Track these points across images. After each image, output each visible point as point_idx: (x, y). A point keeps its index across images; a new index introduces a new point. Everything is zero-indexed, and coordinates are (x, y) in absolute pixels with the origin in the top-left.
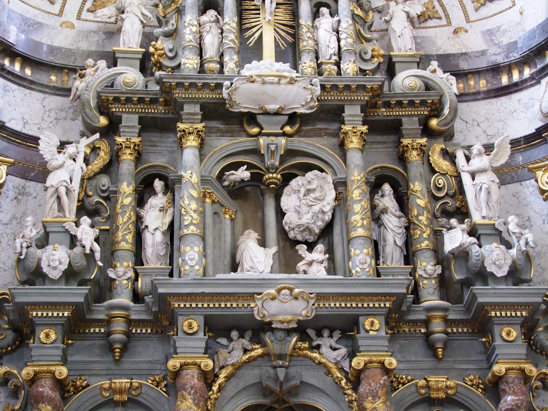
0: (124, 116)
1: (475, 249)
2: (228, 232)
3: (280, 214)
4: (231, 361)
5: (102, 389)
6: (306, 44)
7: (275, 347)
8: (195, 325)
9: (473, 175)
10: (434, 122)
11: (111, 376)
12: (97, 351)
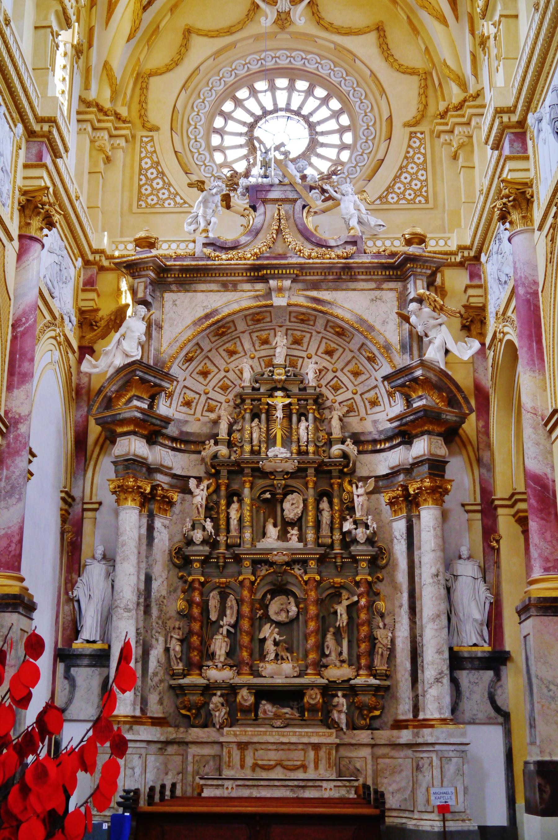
1: (354, 531)
3: (283, 510)
5: (216, 582)
6: (295, 438)
7: (278, 570)
8: (248, 563)
9: (358, 496)
10: (345, 470)
11: (220, 577)
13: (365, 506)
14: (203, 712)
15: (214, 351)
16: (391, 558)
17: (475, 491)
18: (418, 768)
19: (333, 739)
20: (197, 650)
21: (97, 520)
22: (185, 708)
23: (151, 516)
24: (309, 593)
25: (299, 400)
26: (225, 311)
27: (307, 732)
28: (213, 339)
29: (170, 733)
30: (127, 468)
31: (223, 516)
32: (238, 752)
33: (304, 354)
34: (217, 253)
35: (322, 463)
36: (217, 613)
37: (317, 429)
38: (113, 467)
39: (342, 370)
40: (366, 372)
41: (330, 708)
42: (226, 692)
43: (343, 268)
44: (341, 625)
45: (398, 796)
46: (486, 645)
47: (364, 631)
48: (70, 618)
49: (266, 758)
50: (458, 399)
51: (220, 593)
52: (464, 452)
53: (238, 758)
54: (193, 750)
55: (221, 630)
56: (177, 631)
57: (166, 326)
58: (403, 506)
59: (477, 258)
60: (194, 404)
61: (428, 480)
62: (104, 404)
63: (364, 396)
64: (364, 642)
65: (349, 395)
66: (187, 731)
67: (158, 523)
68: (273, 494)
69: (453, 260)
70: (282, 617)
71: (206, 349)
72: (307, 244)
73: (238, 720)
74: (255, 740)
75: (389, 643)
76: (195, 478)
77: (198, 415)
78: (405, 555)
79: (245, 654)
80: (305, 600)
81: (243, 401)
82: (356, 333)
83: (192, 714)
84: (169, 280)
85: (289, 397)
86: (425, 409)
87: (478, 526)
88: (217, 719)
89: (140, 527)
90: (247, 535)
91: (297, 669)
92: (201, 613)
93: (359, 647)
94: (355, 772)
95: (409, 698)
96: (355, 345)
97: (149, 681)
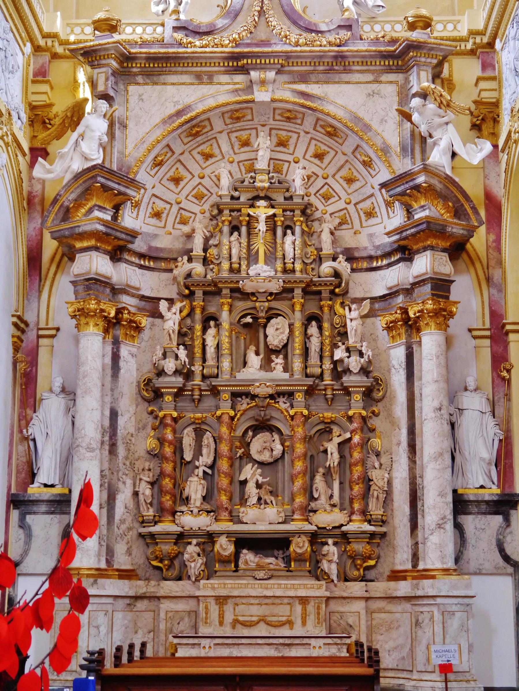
0: (196, 291)
1: (346, 360)
2: (242, 345)
3: (266, 336)
4: (242, 409)
5: (191, 418)
6: (279, 254)
7: (261, 404)
8: (227, 396)
9: (351, 320)
10: (337, 290)
11: (194, 412)
12: (188, 401)
13: (359, 332)
14: (176, 563)
15: (187, 154)
16: (389, 390)
17: (483, 314)
18: (417, 623)
19: (323, 592)
20: (170, 494)
21: (55, 348)
22: (156, 558)
23: (116, 343)
24: (296, 430)
25: (284, 210)
26: (200, 108)
27: (293, 585)
28: (186, 140)
29: (140, 587)
30: (88, 288)
31: (198, 343)
32: (217, 607)
33: (290, 158)
34: (190, 39)
35: (310, 283)
36: (192, 452)
37: (305, 244)
38: (71, 288)
39: (334, 176)
40: (361, 179)
41: (318, 558)
42: (203, 540)
43: (336, 57)
44: (332, 465)
45: (396, 655)
46: (494, 487)
47: (357, 471)
48: (24, 460)
49: (247, 614)
50: (466, 210)
51: (195, 430)
52: (472, 270)
53: (217, 613)
54: (166, 606)
55: (196, 471)
56: (146, 472)
57: (131, 124)
58: (403, 331)
59: (491, 45)
60: (164, 216)
61: (430, 302)
62: (61, 215)
63: (359, 206)
64: (358, 484)
65: (341, 205)
66: (159, 585)
67: (124, 351)
68: (255, 318)
69: (463, 47)
70: (266, 457)
71: (178, 152)
72: (293, 28)
73: (216, 572)
74: (235, 593)
75: (386, 485)
76: (166, 299)
77: (169, 227)
78: (404, 386)
79: (224, 498)
80: (291, 437)
81: (220, 211)
82: (350, 133)
83: (165, 565)
84: (135, 70)
85: (273, 207)
86: (428, 222)
87: (486, 354)
88: (193, 571)
89: (104, 356)
90: (226, 364)
91: (283, 514)
92: (175, 453)
93: (351, 489)
94: (348, 628)
95: (408, 546)
96: (348, 147)
97: (116, 529)
